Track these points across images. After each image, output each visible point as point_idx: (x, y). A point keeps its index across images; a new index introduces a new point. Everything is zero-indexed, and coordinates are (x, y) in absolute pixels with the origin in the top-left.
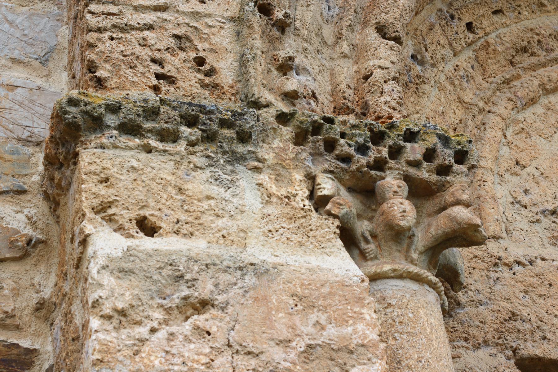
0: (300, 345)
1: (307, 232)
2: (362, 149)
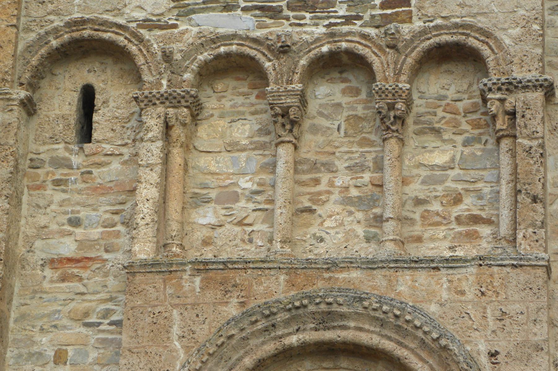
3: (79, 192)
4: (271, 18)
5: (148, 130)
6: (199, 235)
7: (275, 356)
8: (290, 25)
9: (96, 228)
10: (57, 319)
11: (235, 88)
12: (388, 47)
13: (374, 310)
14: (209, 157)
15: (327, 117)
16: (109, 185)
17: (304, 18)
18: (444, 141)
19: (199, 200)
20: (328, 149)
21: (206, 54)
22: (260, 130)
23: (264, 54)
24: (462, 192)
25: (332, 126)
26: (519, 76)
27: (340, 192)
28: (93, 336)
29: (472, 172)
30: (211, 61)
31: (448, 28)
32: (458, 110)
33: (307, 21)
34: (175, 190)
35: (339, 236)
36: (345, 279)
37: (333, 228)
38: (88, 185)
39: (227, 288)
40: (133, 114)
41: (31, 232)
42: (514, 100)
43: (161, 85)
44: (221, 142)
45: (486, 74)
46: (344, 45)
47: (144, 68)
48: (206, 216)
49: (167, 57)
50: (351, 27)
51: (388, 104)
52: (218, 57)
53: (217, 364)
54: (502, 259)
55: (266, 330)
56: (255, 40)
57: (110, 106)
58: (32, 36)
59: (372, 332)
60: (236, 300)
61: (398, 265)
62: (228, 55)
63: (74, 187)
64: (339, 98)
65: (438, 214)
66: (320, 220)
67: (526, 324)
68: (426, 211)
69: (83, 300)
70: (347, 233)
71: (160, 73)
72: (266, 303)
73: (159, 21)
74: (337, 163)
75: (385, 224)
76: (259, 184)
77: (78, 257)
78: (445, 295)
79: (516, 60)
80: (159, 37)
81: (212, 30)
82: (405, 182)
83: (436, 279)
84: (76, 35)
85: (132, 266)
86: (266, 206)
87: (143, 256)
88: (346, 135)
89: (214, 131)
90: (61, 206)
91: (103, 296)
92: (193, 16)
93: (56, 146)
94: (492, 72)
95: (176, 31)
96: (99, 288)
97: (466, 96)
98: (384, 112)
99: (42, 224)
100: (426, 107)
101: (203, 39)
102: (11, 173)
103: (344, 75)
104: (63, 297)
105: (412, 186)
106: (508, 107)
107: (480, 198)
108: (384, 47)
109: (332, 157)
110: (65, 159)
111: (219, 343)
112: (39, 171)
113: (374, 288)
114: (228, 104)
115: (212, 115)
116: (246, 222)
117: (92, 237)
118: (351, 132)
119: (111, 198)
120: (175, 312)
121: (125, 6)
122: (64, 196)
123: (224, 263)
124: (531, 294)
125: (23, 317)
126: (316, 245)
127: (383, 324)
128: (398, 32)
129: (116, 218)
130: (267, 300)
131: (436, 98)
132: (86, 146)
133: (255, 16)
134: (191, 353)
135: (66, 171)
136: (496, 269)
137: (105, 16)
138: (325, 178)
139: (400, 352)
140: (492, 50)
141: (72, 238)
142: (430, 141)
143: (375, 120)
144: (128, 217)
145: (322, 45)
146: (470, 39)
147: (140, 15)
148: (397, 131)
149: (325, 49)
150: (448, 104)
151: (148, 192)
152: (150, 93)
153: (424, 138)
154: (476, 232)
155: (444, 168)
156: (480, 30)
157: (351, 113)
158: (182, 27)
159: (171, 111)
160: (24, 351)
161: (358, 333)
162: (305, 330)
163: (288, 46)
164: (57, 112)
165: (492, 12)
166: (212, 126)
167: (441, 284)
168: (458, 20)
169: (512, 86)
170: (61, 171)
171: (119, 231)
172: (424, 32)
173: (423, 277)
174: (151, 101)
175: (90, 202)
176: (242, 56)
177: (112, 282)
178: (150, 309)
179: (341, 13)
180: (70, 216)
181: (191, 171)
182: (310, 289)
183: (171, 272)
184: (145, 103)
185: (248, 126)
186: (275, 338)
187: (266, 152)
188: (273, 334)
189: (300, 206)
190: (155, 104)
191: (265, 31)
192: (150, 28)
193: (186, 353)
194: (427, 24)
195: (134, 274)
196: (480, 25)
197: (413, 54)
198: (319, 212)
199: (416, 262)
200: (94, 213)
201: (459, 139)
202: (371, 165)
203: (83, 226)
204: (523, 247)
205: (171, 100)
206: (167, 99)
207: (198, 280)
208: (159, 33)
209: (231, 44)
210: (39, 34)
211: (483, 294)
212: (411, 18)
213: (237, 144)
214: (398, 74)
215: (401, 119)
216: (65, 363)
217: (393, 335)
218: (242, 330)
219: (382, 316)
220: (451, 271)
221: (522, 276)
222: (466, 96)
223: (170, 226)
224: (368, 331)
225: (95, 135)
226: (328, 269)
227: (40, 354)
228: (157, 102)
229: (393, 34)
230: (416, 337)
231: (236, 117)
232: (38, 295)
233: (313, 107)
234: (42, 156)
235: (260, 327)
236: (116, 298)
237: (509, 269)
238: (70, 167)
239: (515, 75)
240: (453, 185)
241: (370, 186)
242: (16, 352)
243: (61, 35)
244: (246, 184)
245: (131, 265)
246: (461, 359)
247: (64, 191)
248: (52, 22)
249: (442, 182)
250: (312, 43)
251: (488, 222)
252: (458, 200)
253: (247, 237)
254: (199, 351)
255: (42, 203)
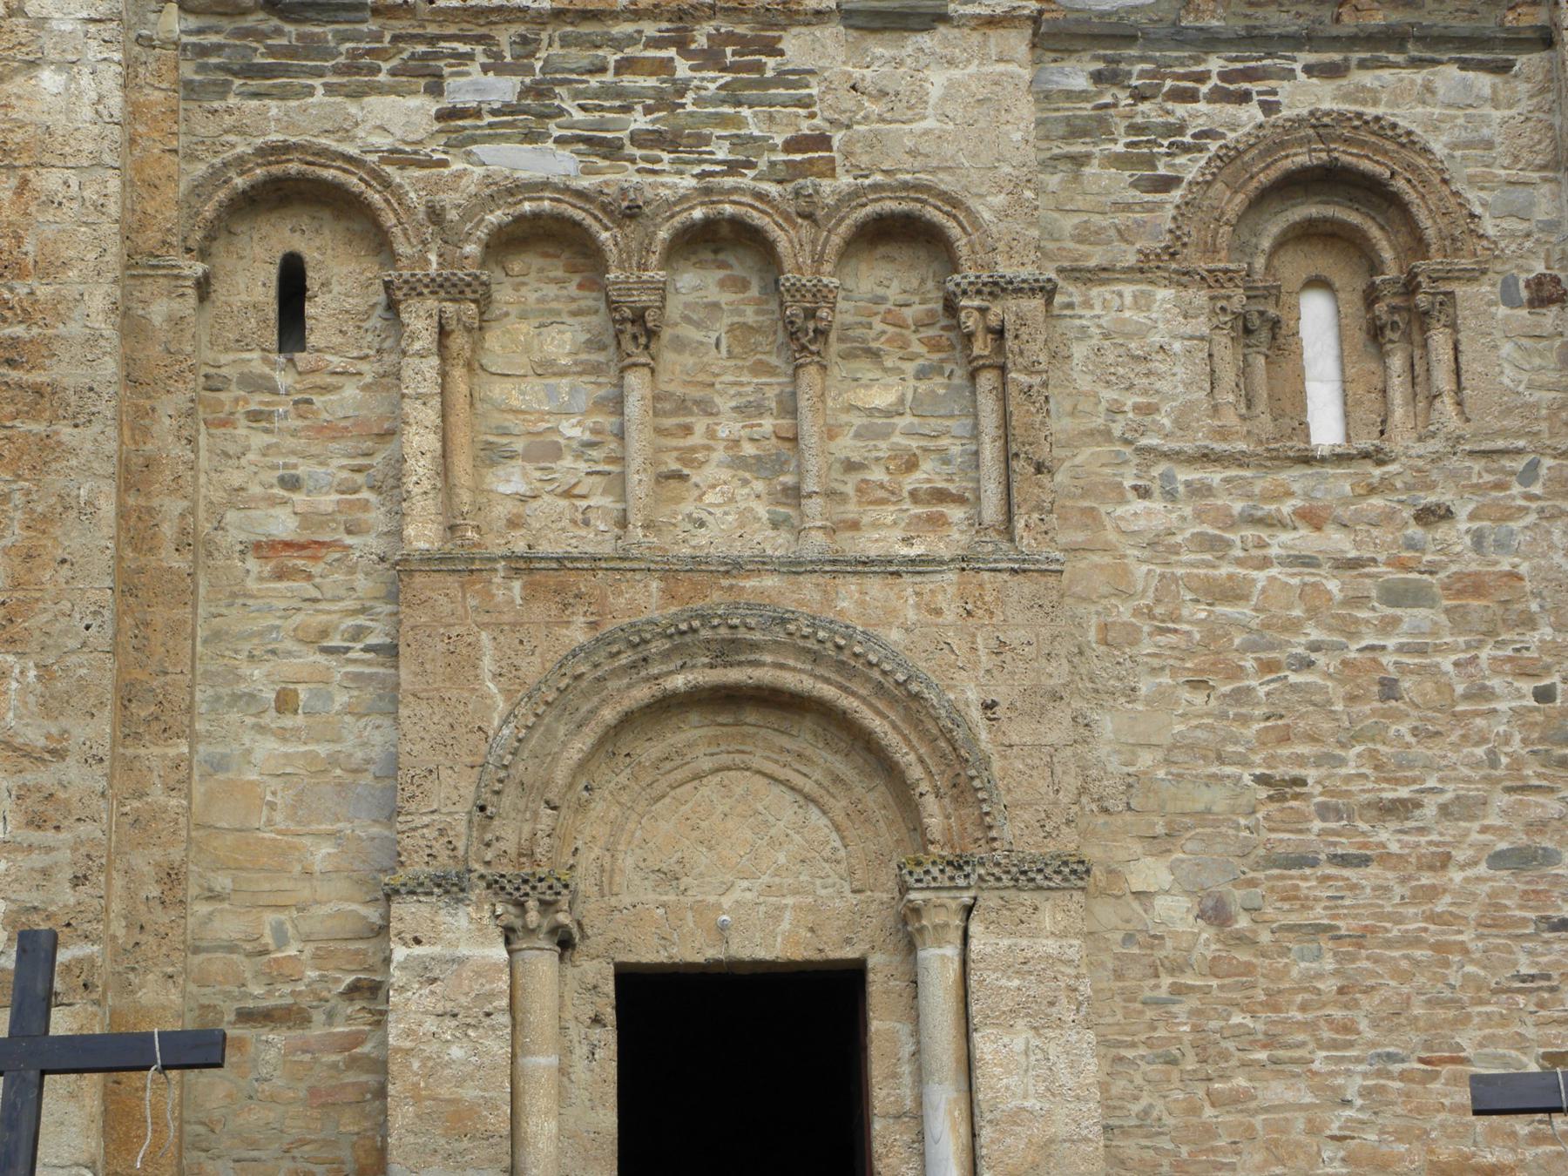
0: (473, 995)
1: (485, 936)
2: (518, 889)
3: (294, 433)
4: (605, 157)
5: (413, 337)
6: (501, 511)
7: (648, 706)
8: (638, 171)
9: (327, 493)
10: (275, 640)
11: (541, 270)
12: (799, 215)
13: (805, 637)
14: (508, 384)
15: (698, 325)
16: (343, 424)
17: (660, 160)
18: (886, 370)
19: (492, 455)
20: (702, 377)
21: (499, 213)
22: (588, 341)
23: (596, 217)
24: (918, 452)
25: (705, 340)
26: (1009, 273)
27: (726, 448)
28: (339, 670)
29: (932, 421)
30: (508, 224)
31: (892, 189)
32: (904, 320)
33: (667, 167)
34: (461, 438)
35: (730, 518)
36: (754, 588)
37: (718, 505)
38: (307, 422)
39: (566, 600)
40: (373, 306)
41: (218, 496)
42: (1003, 310)
43: (428, 262)
44: (525, 360)
45: (953, 265)
46: (729, 209)
47: (397, 231)
48: (510, 481)
49: (435, 215)
50: (740, 180)
51: (805, 310)
52: (520, 219)
53: (558, 718)
54: (995, 561)
55: (633, 666)
56: (581, 194)
57: (334, 292)
58: (200, 169)
59: (801, 671)
60: (582, 619)
61: (837, 568)
62: (536, 216)
63: (284, 424)
64: (714, 294)
65: (882, 486)
66: (696, 493)
67: (1036, 660)
68: (863, 481)
69: (317, 611)
70: (741, 513)
71: (424, 243)
72: (632, 625)
73: (416, 152)
74: (717, 400)
75: (803, 501)
76: (594, 431)
77: (302, 540)
78: (912, 615)
79: (1001, 246)
80: (418, 180)
81: (507, 172)
82: (831, 433)
83: (896, 589)
84: (276, 170)
85: (406, 560)
86: (608, 468)
87: (423, 545)
88: (731, 355)
89: (513, 341)
90: (264, 455)
91: (349, 604)
92: (474, 148)
93: (247, 355)
94: (965, 264)
95: (446, 171)
96: (342, 592)
97: (917, 299)
98: (799, 322)
99: (236, 485)
100: (855, 314)
101: (494, 188)
102: (192, 401)
103: (721, 256)
104: (282, 604)
105: (840, 441)
106: (993, 321)
107: (946, 462)
108: (794, 215)
109: (708, 391)
110: (262, 376)
111: (562, 685)
112: (222, 395)
113: (801, 603)
114: (532, 297)
115: (507, 314)
116: (576, 492)
117: (322, 508)
118: (737, 350)
119: (350, 445)
120: (484, 635)
121: (357, 124)
122: (268, 439)
123: (558, 560)
124: (1041, 614)
125: (216, 636)
126: (694, 531)
127: (816, 658)
128: (817, 192)
129: (360, 478)
130: (633, 620)
131: (870, 301)
132: (298, 356)
133: (578, 153)
134: (516, 700)
135: (267, 398)
136: (986, 575)
137: (324, 141)
138: (700, 424)
139: (847, 702)
140: (963, 228)
141: (289, 509)
142: (865, 369)
143: (775, 333)
144: (380, 477)
145: (692, 208)
146: (929, 209)
147: (384, 142)
148: (818, 353)
149: (698, 214)
150: (889, 311)
151: (420, 440)
152: (413, 275)
153: (855, 364)
154: (942, 515)
155: (888, 413)
156: (945, 196)
157: (736, 319)
158: (457, 166)
159: (450, 307)
160: (225, 691)
161: (778, 672)
162: (694, 666)
163: (639, 207)
164: (244, 297)
165: (960, 166)
166: (508, 331)
167: (905, 598)
168: (908, 177)
169: (998, 288)
170: (258, 397)
171: (367, 501)
172: (855, 193)
173: (875, 587)
174: (414, 289)
175: (313, 450)
176: (559, 219)
177: (361, 582)
178: (442, 630)
179: (720, 156)
180: (281, 472)
181: (478, 405)
182: (702, 603)
183: (472, 571)
184: (405, 290)
185: (568, 335)
186: (647, 680)
187: (601, 380)
188: (643, 673)
189: (663, 469)
190: (420, 294)
191: (596, 180)
192: (403, 165)
193: (507, 700)
194: (859, 181)
195: (411, 573)
196: (942, 187)
197: (842, 229)
198: (695, 479)
199: (865, 563)
200: (322, 469)
201: (910, 367)
202: (774, 405)
203: (304, 490)
204: (1025, 542)
205: (445, 287)
206: (441, 286)
207: (517, 585)
208: (418, 173)
209: (541, 199)
210: (212, 166)
211: (969, 613)
212: (834, 169)
213: (552, 363)
214: (818, 260)
215: (821, 334)
216: (295, 712)
217: (833, 676)
218: (596, 666)
219: (816, 647)
220: (918, 579)
221: (1024, 587)
222: (917, 299)
223: (458, 495)
224: (794, 669)
225: (312, 339)
226: (727, 572)
227: (252, 696)
228: (426, 291)
229: (810, 196)
230: (868, 679)
231: (547, 318)
232: (240, 601)
233: (674, 308)
234: (224, 371)
235: (624, 662)
236: (371, 608)
237: (1006, 576)
238: (274, 391)
239: (1001, 270)
240: (904, 441)
241: (774, 440)
242: (210, 692)
243: (250, 170)
244: (572, 430)
245: (406, 560)
246: (943, 712)
247: (266, 431)
248: (233, 146)
249: (886, 435)
250: (675, 204)
251: (960, 500)
252: (911, 465)
253: (580, 517)
254: (530, 698)
255: (232, 449)
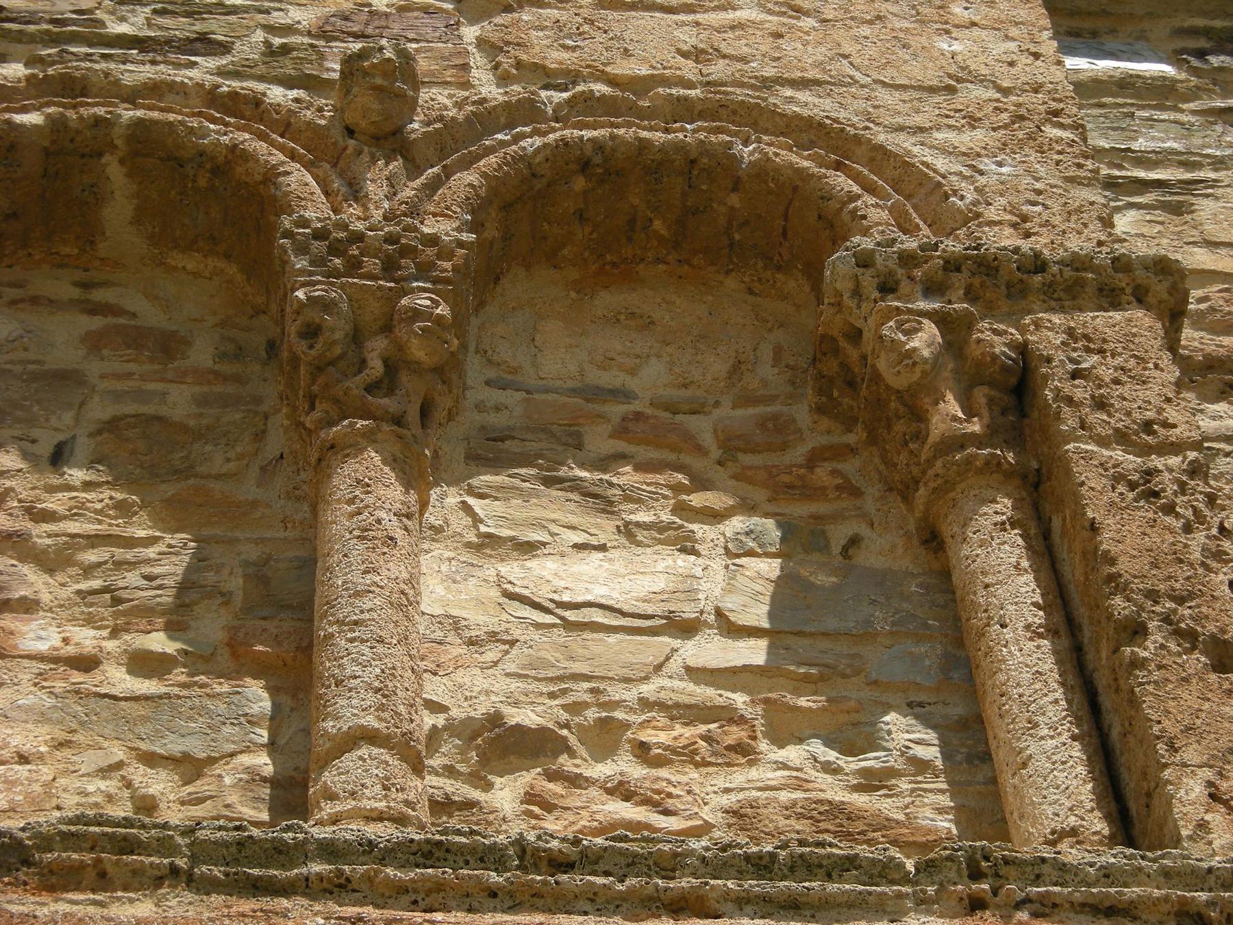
131: (574, 392)
143: (260, 436)
199: (560, 864)
202: (235, 583)
